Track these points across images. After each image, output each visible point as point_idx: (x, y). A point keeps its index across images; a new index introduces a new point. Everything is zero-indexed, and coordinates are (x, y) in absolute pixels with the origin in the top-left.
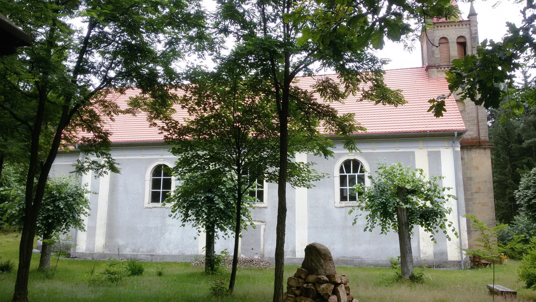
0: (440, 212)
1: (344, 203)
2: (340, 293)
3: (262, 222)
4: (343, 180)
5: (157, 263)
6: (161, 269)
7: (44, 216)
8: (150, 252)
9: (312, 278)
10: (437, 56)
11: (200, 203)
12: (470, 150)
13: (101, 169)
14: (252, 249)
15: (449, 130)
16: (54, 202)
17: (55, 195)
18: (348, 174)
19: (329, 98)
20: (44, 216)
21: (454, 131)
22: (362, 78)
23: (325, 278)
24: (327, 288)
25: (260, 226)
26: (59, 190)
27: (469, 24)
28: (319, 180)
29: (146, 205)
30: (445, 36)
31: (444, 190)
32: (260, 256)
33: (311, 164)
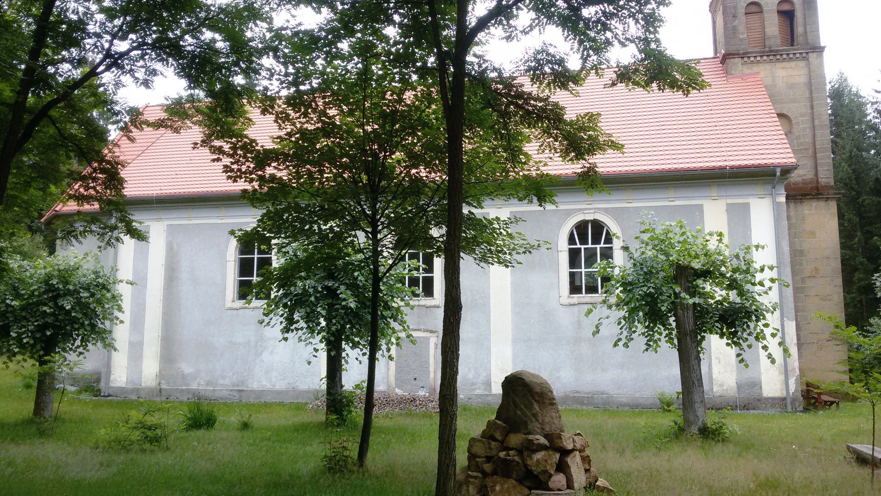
0: (756, 310)
1: (576, 298)
2: (573, 470)
3: (431, 332)
4: (574, 256)
5: (248, 405)
6: (247, 416)
7: (36, 324)
8: (238, 385)
9: (515, 439)
10: (741, 37)
11: (312, 299)
12: (801, 203)
13: (110, 233)
14: (415, 379)
15: (766, 166)
16: (55, 298)
17: (56, 286)
18: (583, 247)
19: (549, 84)
20: (36, 324)
22: (616, 36)
23: (543, 440)
24: (546, 461)
25: (428, 339)
26: (64, 278)
28: (530, 252)
29: (229, 304)
31: (762, 270)
32: (428, 391)
33: (513, 220)
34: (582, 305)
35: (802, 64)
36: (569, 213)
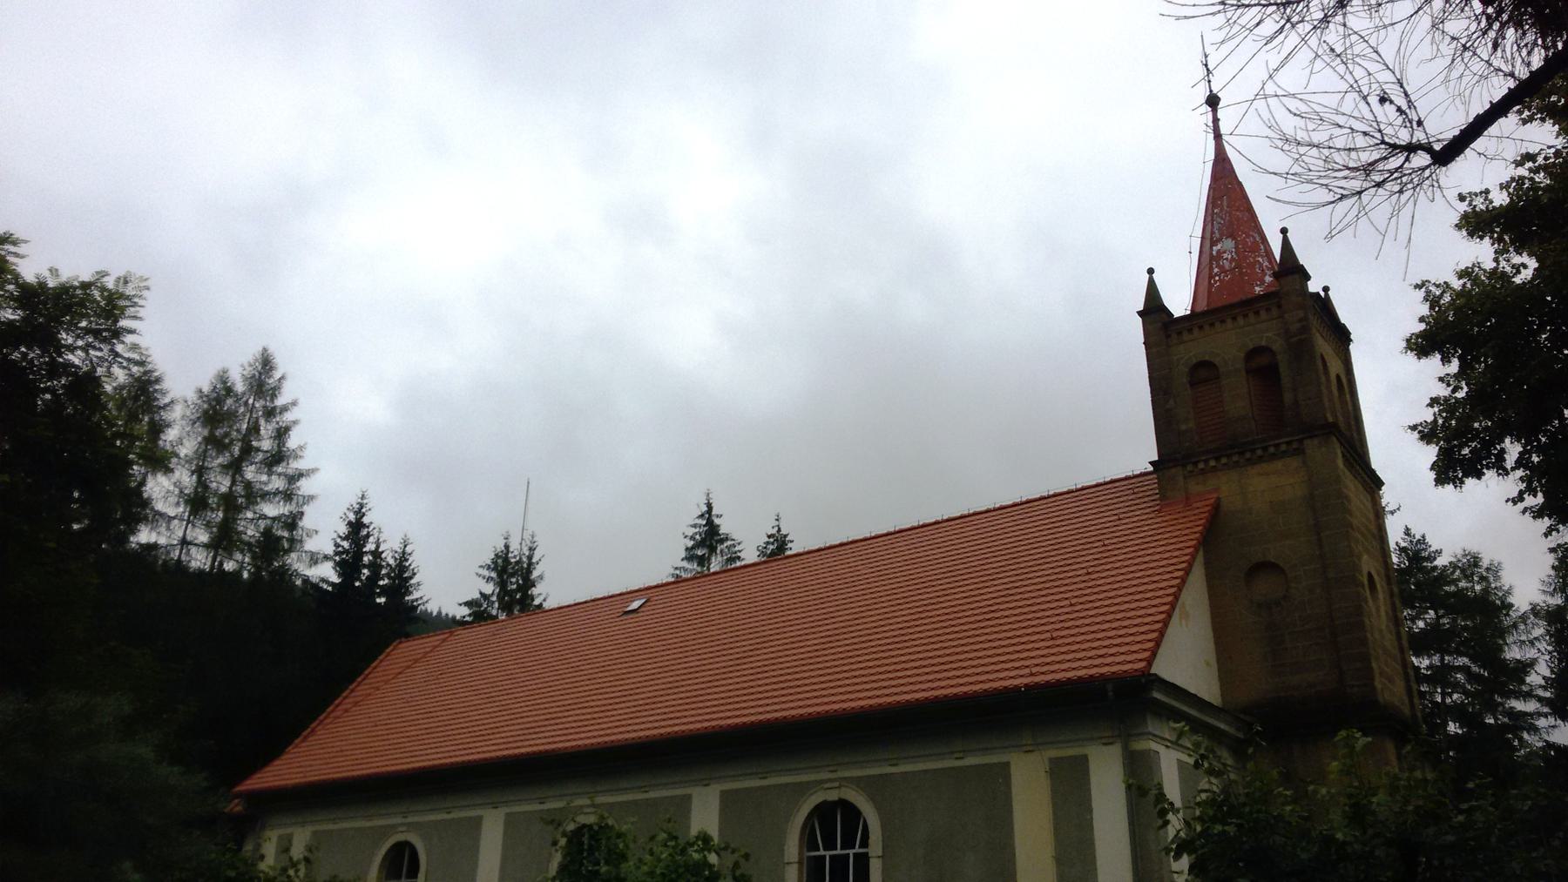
10: (1183, 427)
18: (828, 854)
27: (1279, 307)
30: (1207, 358)
35: (1294, 463)
36: (803, 789)
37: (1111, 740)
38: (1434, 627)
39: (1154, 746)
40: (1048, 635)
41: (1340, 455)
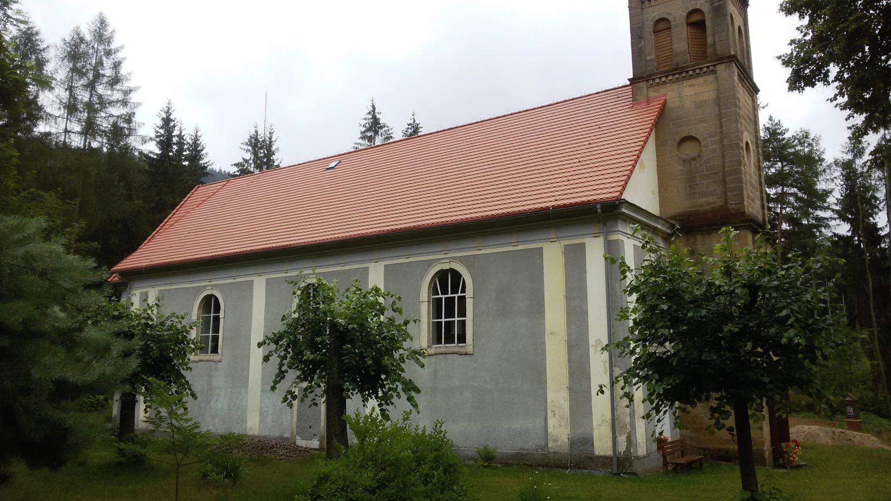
10: (648, 58)
18: (444, 296)
21: (595, 202)
34: (438, 356)
35: (710, 78)
36: (430, 263)
37: (598, 235)
38: (781, 172)
39: (620, 237)
40: (566, 179)
41: (736, 74)
